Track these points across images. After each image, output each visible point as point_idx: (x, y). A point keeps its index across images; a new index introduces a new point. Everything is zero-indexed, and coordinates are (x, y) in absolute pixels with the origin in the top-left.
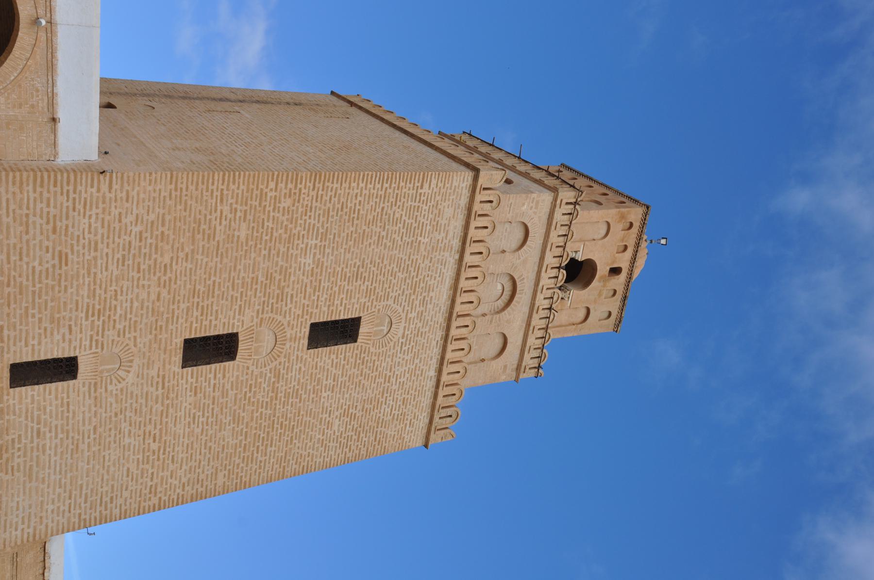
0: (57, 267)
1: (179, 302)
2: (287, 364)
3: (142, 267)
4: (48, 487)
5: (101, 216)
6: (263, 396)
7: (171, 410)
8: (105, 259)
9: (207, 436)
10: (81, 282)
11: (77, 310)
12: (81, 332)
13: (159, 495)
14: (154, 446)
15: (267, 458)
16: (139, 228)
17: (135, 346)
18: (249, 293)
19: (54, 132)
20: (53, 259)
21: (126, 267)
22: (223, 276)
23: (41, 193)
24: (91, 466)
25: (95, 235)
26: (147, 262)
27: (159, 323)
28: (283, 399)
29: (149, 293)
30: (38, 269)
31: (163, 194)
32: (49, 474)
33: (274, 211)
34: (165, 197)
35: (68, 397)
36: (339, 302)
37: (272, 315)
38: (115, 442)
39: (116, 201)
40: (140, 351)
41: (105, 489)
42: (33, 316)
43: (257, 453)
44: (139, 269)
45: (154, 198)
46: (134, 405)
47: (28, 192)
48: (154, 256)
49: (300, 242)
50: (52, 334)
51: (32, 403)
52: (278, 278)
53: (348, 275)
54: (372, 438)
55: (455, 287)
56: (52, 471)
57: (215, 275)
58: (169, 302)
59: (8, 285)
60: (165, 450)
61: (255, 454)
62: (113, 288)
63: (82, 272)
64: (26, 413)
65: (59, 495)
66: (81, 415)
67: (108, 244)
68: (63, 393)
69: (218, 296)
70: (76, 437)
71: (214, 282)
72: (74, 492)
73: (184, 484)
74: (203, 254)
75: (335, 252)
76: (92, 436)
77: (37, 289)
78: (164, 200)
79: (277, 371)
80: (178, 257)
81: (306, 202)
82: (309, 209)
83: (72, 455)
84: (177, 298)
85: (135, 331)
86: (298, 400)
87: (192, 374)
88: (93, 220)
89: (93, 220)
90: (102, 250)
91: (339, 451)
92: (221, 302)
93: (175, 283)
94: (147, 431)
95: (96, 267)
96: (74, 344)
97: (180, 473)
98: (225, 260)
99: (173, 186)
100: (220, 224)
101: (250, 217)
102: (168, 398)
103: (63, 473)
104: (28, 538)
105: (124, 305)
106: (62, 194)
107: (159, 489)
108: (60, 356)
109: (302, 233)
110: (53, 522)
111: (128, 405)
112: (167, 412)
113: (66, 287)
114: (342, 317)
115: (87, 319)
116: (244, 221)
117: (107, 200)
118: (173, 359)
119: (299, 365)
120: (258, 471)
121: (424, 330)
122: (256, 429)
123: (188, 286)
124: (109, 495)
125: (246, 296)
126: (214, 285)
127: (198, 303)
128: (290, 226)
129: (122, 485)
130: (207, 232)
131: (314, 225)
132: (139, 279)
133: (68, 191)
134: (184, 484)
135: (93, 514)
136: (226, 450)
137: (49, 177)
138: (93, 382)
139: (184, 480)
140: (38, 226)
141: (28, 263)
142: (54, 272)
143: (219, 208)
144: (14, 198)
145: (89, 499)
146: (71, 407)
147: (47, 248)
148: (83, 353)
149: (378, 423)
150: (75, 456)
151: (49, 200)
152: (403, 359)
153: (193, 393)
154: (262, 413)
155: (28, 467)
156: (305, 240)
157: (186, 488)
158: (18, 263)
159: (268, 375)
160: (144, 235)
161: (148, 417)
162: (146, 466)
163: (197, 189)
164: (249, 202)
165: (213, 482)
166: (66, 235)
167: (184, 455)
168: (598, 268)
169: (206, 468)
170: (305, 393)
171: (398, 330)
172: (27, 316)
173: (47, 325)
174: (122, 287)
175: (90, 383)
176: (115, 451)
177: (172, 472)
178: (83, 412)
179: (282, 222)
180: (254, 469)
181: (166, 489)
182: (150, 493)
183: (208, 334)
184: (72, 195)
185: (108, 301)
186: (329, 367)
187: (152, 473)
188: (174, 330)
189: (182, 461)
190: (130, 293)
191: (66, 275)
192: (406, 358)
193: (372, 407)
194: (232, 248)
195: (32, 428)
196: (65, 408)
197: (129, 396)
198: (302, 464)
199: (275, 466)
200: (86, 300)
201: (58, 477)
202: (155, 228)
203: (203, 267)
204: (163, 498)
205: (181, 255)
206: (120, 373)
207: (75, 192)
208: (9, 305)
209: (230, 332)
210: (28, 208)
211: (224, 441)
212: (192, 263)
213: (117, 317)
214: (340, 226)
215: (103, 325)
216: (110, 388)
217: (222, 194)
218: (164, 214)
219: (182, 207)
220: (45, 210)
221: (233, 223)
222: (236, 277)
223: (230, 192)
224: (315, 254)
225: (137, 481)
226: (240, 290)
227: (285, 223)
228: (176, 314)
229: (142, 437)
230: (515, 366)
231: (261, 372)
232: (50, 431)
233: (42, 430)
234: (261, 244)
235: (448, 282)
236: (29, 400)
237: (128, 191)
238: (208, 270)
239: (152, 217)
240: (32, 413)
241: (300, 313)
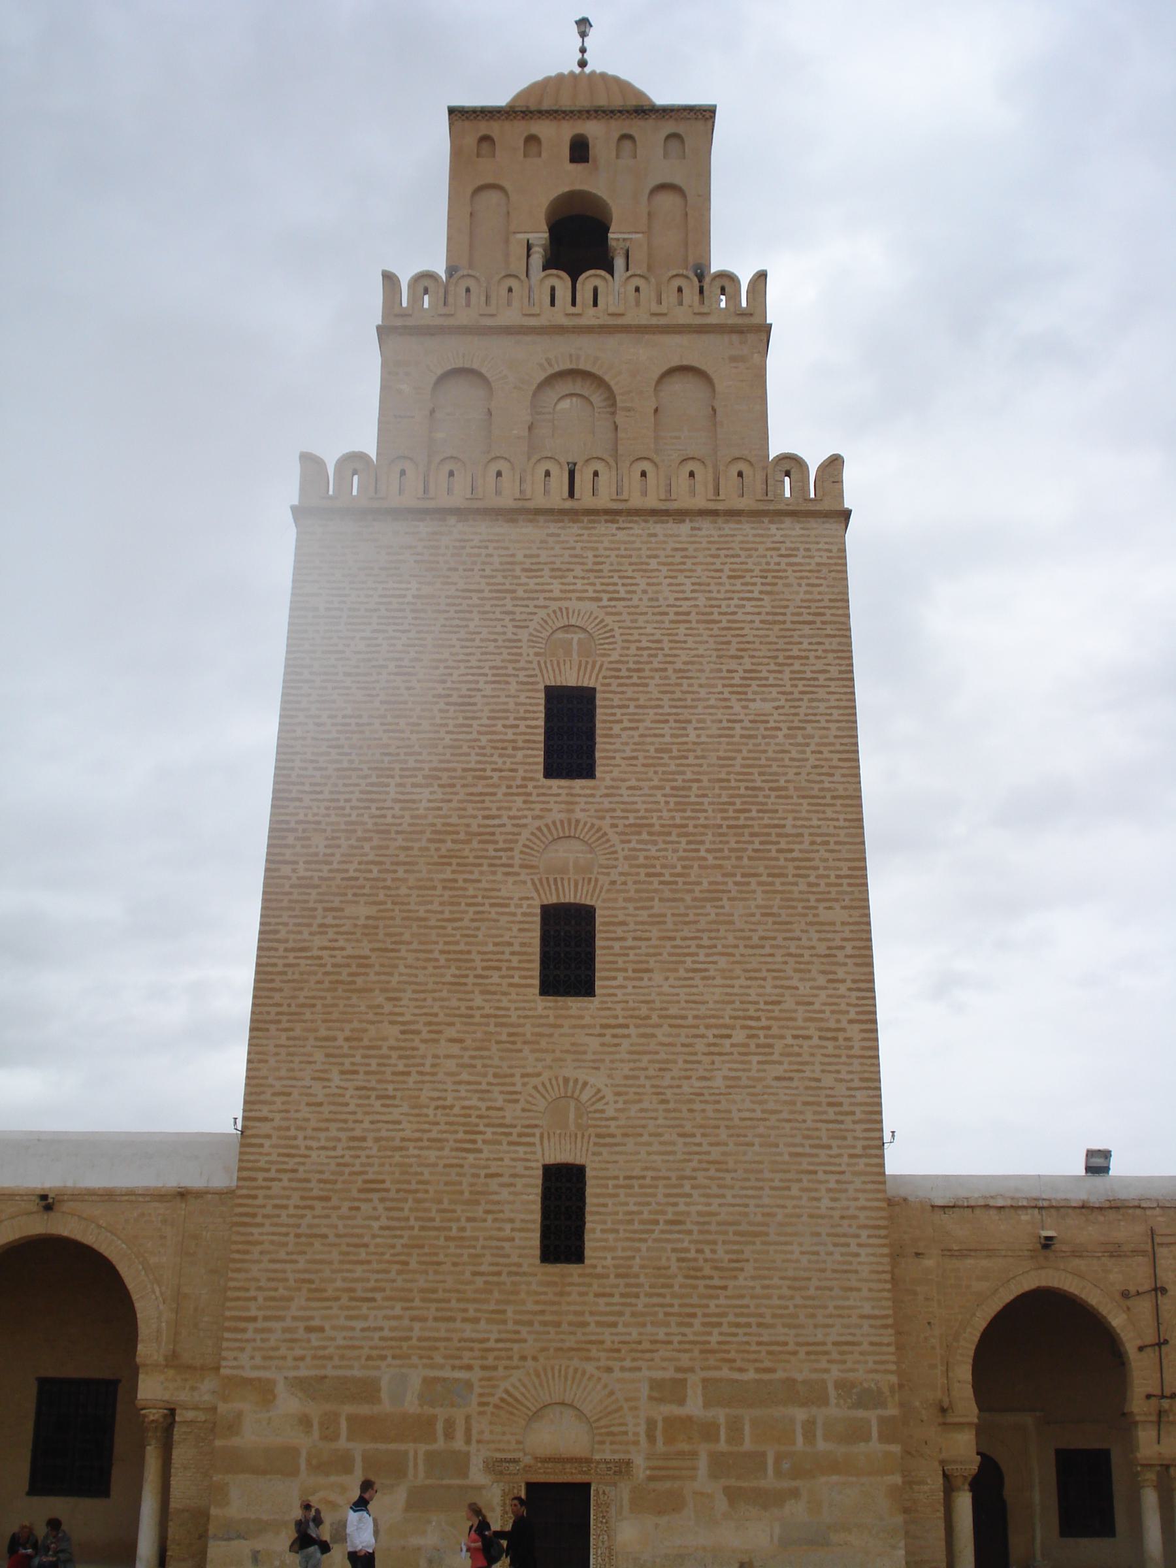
0: (384, 1194)
1: (471, 1008)
2: (619, 813)
3: (401, 1068)
4: (784, 1207)
5: (309, 1132)
6: (675, 851)
7: (671, 1012)
8: (379, 1125)
9: (736, 946)
10: (413, 1160)
11: (461, 1166)
12: (502, 1159)
13: (844, 1024)
14: (739, 1036)
15: (806, 831)
16: (335, 1076)
17: (539, 1075)
18: (471, 892)
19: (199, 1194)
20: (370, 1200)
21: (399, 1094)
22: (434, 938)
23: (265, 1216)
24: (757, 1140)
25: (339, 1140)
26: (393, 1061)
27: (504, 1038)
28: (689, 814)
29: (447, 1057)
30: (384, 1222)
31: (283, 1041)
32: (757, 1206)
33: (331, 863)
34: (288, 1039)
35: (616, 1178)
36: (510, 731)
37: (518, 847)
38: (718, 1102)
39: (287, 1111)
40: (551, 1067)
41: (809, 1116)
42: (463, 1229)
43: (792, 851)
44: (403, 1073)
45: (288, 1054)
46: (651, 1072)
47: (261, 1234)
48: (384, 1051)
49: (389, 813)
50: (498, 1203)
51: (617, 1231)
52: (449, 845)
53: (461, 721)
54: (806, 629)
56: (752, 1202)
57: (431, 951)
58: (466, 1024)
59: (406, 1263)
60: (751, 1018)
61: (794, 855)
62: (431, 1112)
63: (397, 1159)
64: (632, 1240)
65: (803, 1190)
66: (655, 1157)
67: (356, 1121)
68: (606, 1186)
69: (467, 944)
70: (695, 1164)
71: (442, 952)
72: (805, 1167)
73: (830, 981)
74: (391, 974)
75: (417, 749)
76: (698, 1140)
77: (417, 1224)
78: (294, 1039)
79: (628, 830)
80: (391, 1014)
81: (324, 811)
82: (333, 804)
83: (727, 1171)
84: (463, 1011)
85: (512, 1075)
86: (695, 785)
87: (607, 979)
88: (314, 1144)
89: (314, 1144)
90: (364, 1130)
91: (821, 693)
92: (480, 938)
93: (436, 1015)
94: (706, 1050)
95: (393, 1139)
96: (520, 1169)
97: (804, 988)
98: (407, 937)
99: (273, 1027)
100: (343, 949)
102: (648, 1017)
103: (760, 1184)
104: (879, 1237)
105: (463, 1094)
106: (269, 1188)
107: (832, 1025)
108: (539, 1190)
109: (374, 811)
110: (856, 1199)
111: (648, 1083)
112: (675, 1017)
113: (419, 1182)
114: (541, 723)
115: (480, 1151)
116: (342, 910)
117: (285, 1124)
118: (573, 1012)
119: (623, 791)
120: (832, 846)
121: (591, 560)
122: (740, 858)
123: (444, 994)
124: (824, 1108)
125: (475, 897)
126: (449, 952)
127: (476, 976)
128: (359, 834)
129: (807, 1088)
130: (354, 969)
131: (362, 792)
132: (421, 1073)
133: (265, 1179)
134: (830, 981)
135: (859, 1134)
136: (775, 910)
137: (240, 1205)
138: (593, 1139)
139: (822, 980)
140: (316, 1221)
141: (374, 1236)
142: (393, 1200)
143: (316, 953)
144: (269, 1252)
145: (824, 1141)
146: (634, 1174)
147: (351, 1209)
148: (539, 1156)
149: (775, 622)
150: (731, 1165)
151: (276, 1206)
152: (645, 592)
153: (646, 976)
154: (708, 851)
155: (737, 1238)
156: (388, 804)
157: (841, 975)
158: (372, 1249)
159: (633, 845)
160: (347, 1067)
161: (679, 1049)
162: (779, 1045)
163: (281, 990)
164: (311, 905)
165: (838, 928)
166: (335, 1182)
167: (769, 983)
168: (567, 189)
169: (804, 942)
170: (683, 773)
172: (462, 1238)
173: (481, 1209)
174: (432, 1099)
175: (595, 1144)
176: (735, 1102)
177: (798, 1003)
178: (649, 1154)
179: (352, 847)
180: (827, 855)
181: (833, 1012)
182: (835, 1039)
183: (537, 958)
184: (272, 1174)
185: (452, 1119)
186: (635, 733)
187: (795, 1037)
188: (520, 1012)
189: (782, 987)
190: (441, 1086)
191: (399, 1182)
192: (643, 586)
193: (735, 640)
194: (386, 927)
195: (662, 1232)
196: (635, 1182)
197: (631, 1082)
198: (835, 763)
199: (829, 814)
200: (446, 1152)
201: (767, 1191)
202: (337, 1052)
203: (414, 971)
204: (852, 1016)
205: (388, 1007)
206: (584, 1097)
207: (268, 1170)
208: (439, 1263)
209: (538, 919)
210: (287, 1234)
211: (753, 915)
212: (404, 991)
213: (483, 1105)
214: (369, 747)
215: (493, 1126)
216: (610, 1112)
217: (293, 950)
218: (316, 1039)
219: (307, 1011)
220: (292, 1211)
221: (342, 929)
222: (440, 916)
223: (292, 936)
224: (414, 785)
225: (806, 1063)
226: (463, 907)
227: (353, 842)
228: (492, 1012)
229: (717, 1058)
230: (735, 338)
231: (626, 858)
232: (675, 1204)
233: (670, 1217)
234: (385, 880)
236: (611, 1236)
237: (274, 1094)
238: (421, 963)
239: (319, 1056)
240: (635, 1232)
241: (520, 799)
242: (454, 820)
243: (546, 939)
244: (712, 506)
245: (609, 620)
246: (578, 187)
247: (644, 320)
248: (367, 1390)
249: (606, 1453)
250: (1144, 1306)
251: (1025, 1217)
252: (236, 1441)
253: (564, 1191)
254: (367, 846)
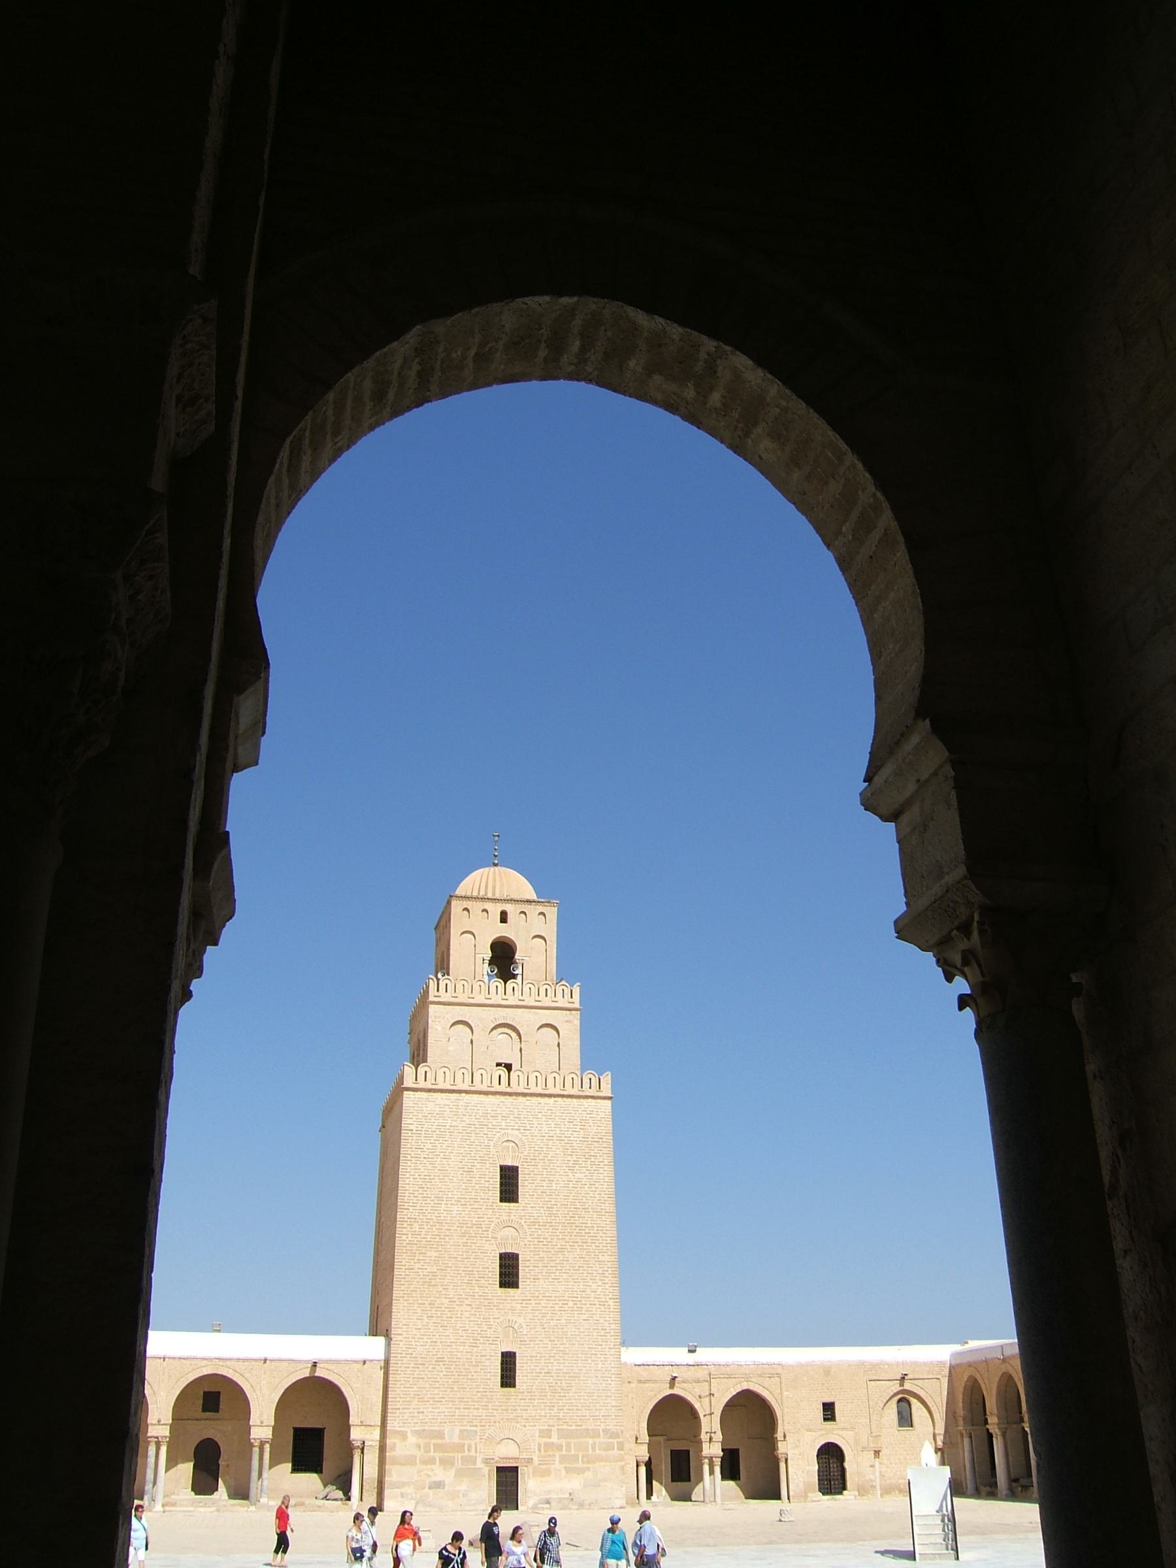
14: (571, 1304)
55: (486, 1093)
97: (594, 1286)
171: (514, 1134)
235: (482, 1098)
239: (419, 1311)
248: (440, 1435)
249: (524, 1456)
250: (707, 1399)
251: (667, 1368)
252: (393, 1453)
253: (508, 1362)
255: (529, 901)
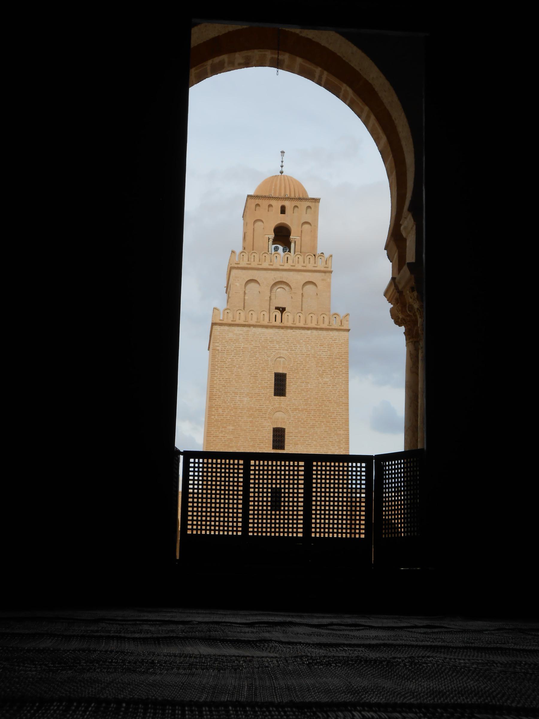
52: (251, 412)
54: (338, 360)
91: (341, 377)
101: (225, 425)
139: (337, 448)
230: (323, 274)
242: (252, 406)
243: (274, 436)
244: (316, 326)
245: (290, 356)
246: (283, 222)
247: (299, 267)
254: (232, 412)
255: (300, 199)
